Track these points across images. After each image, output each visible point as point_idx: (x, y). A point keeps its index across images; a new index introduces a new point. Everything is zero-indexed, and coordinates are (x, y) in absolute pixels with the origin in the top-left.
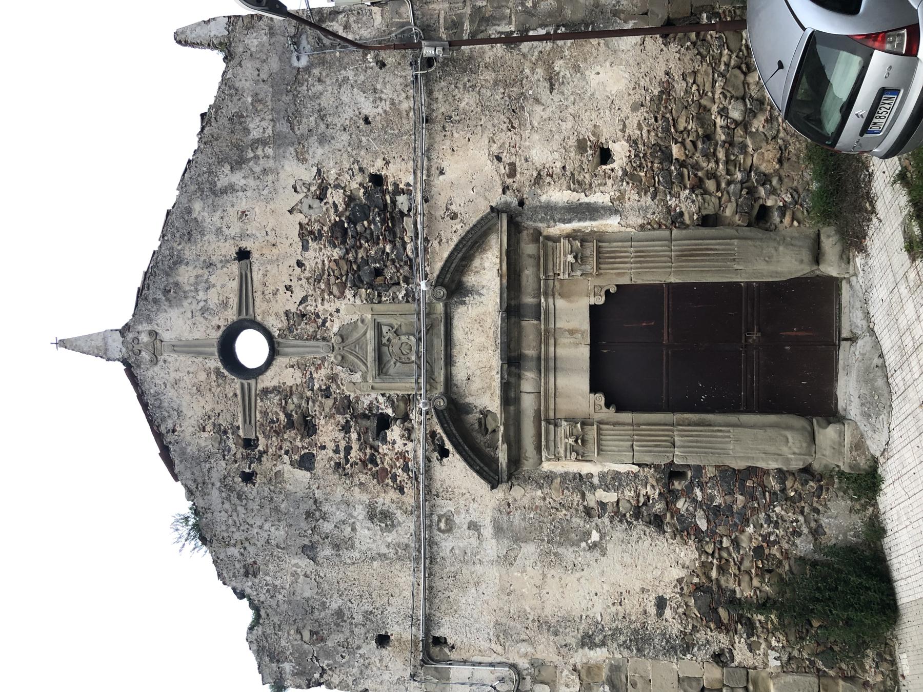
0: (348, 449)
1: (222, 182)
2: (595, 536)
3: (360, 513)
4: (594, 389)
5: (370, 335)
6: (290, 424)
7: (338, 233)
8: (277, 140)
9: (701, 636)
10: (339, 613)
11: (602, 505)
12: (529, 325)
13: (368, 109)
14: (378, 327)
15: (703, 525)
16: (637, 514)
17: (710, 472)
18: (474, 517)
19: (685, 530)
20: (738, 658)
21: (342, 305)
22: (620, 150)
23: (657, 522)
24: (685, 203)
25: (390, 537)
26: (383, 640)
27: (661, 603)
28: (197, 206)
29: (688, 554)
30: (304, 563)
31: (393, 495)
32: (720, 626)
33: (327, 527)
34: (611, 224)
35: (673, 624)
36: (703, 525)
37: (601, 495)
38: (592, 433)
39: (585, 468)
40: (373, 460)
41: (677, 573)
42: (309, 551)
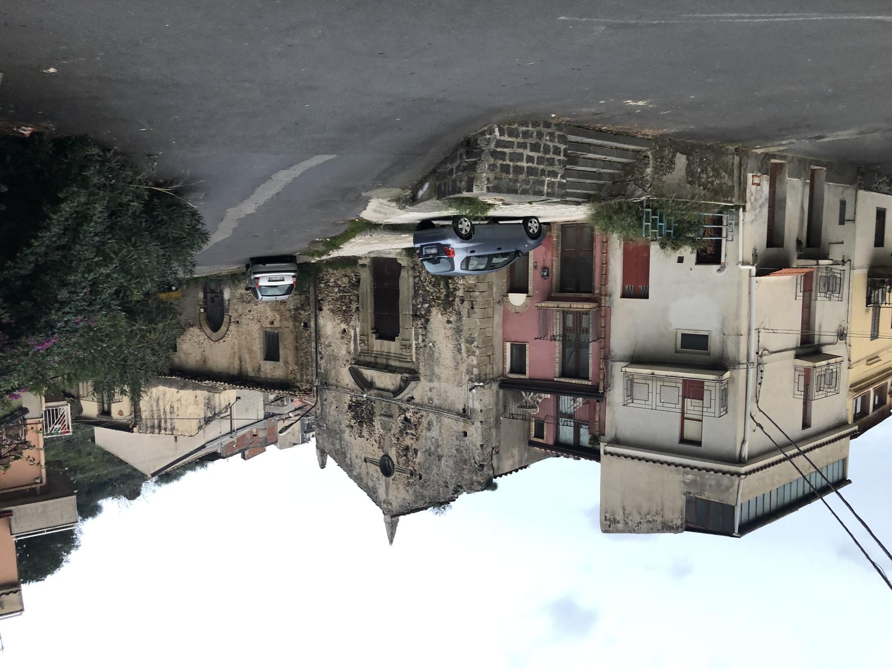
0: (413, 435)
1: (349, 462)
2: (431, 344)
3: (428, 434)
4: (394, 340)
5: (383, 418)
6: (406, 455)
7: (361, 424)
8: (341, 439)
9: (456, 307)
10: (457, 450)
11: (423, 341)
12: (379, 361)
13: (334, 406)
14: (382, 415)
15: (427, 305)
16: (425, 328)
17: (414, 302)
18: (428, 389)
19: (429, 311)
20: (461, 295)
21: (376, 427)
22: (343, 326)
23: (427, 321)
24: (354, 306)
25: (435, 424)
26: (465, 434)
27: (449, 322)
28: (355, 473)
29: (434, 311)
30: (443, 461)
31: (423, 419)
32: (454, 301)
33: (433, 449)
34: (358, 329)
35: (453, 318)
36: (427, 305)
37: (420, 340)
38: (404, 342)
39: (414, 346)
40: (415, 425)
41: (439, 316)
42: (440, 458)
